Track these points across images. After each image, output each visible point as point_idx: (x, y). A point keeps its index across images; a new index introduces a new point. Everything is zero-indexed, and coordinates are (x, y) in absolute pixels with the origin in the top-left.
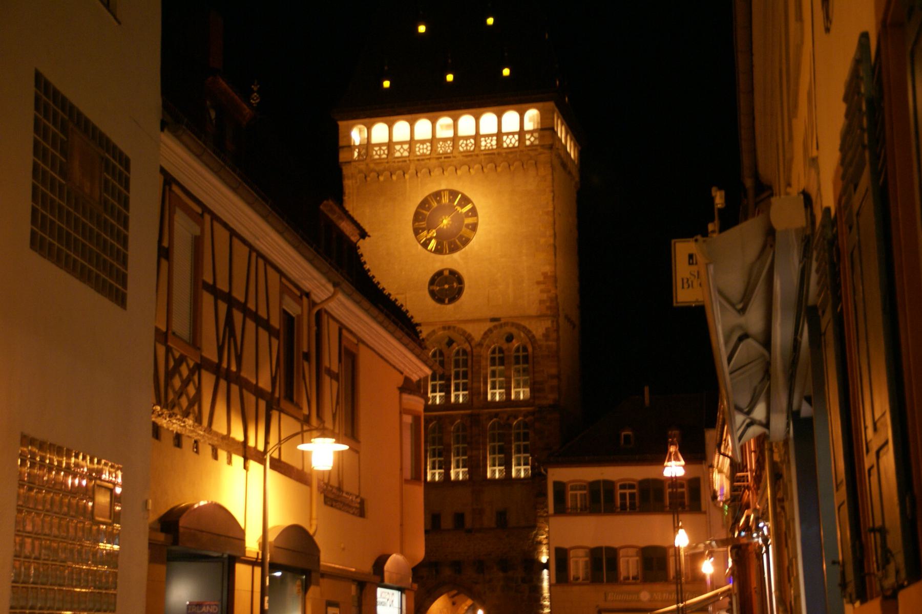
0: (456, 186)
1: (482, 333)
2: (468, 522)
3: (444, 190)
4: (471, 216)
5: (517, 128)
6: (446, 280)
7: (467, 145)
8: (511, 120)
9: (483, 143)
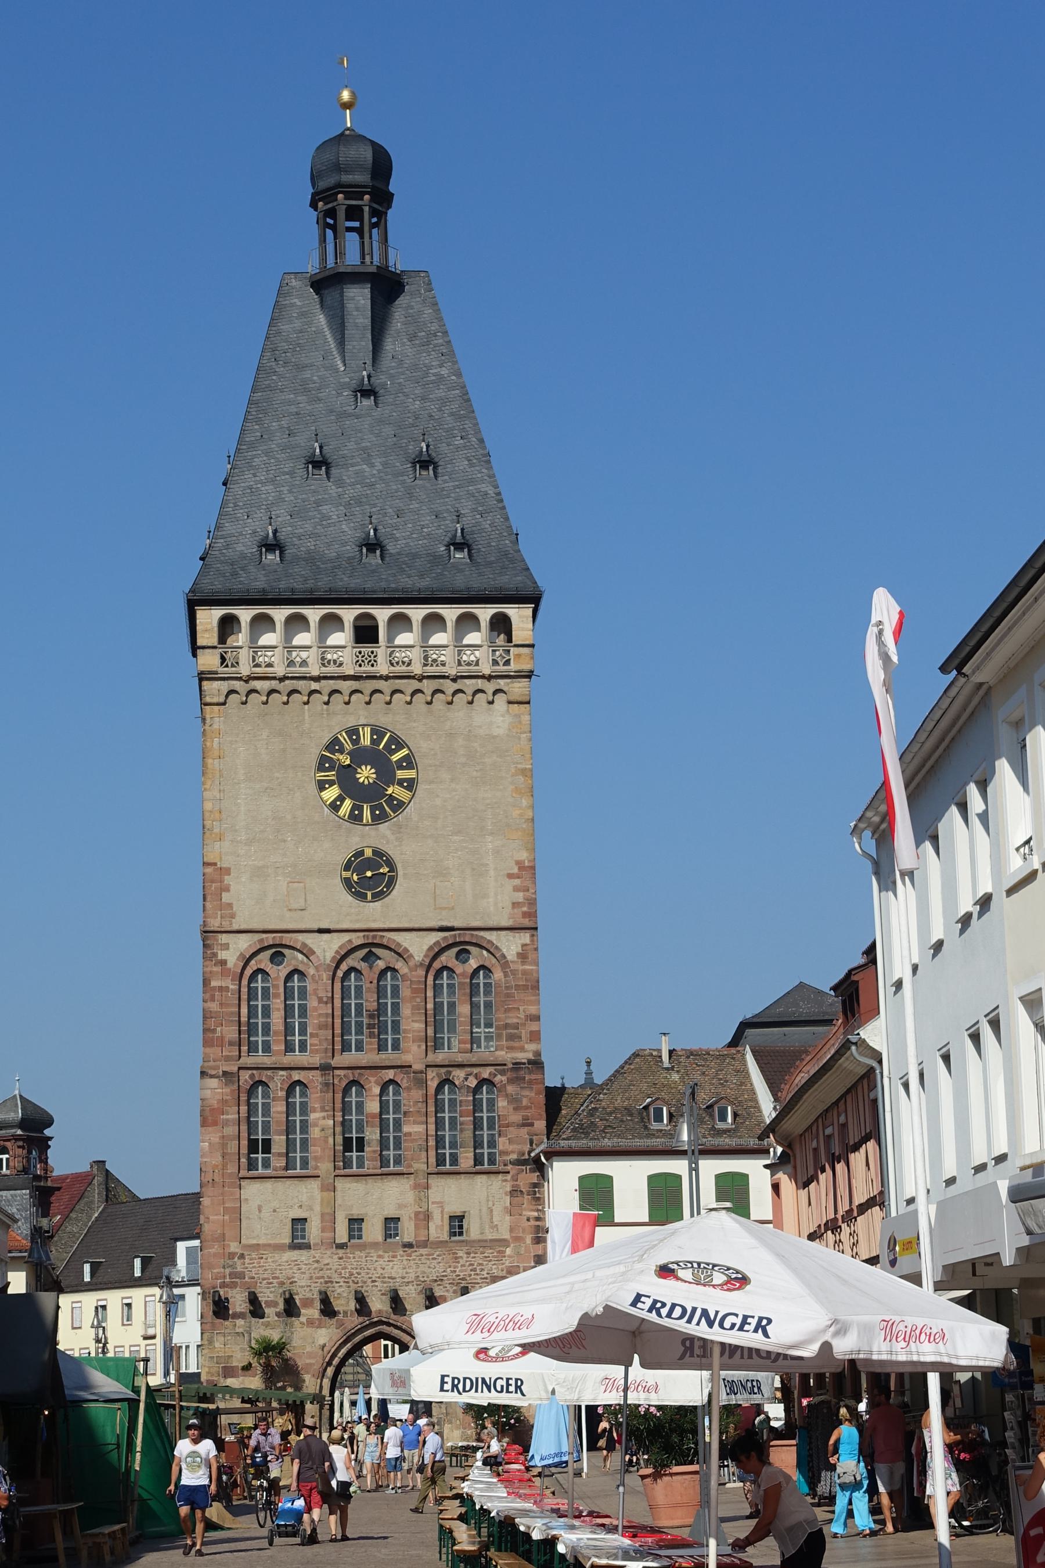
0: (384, 720)
1: (425, 948)
2: (408, 1231)
6: (370, 864)
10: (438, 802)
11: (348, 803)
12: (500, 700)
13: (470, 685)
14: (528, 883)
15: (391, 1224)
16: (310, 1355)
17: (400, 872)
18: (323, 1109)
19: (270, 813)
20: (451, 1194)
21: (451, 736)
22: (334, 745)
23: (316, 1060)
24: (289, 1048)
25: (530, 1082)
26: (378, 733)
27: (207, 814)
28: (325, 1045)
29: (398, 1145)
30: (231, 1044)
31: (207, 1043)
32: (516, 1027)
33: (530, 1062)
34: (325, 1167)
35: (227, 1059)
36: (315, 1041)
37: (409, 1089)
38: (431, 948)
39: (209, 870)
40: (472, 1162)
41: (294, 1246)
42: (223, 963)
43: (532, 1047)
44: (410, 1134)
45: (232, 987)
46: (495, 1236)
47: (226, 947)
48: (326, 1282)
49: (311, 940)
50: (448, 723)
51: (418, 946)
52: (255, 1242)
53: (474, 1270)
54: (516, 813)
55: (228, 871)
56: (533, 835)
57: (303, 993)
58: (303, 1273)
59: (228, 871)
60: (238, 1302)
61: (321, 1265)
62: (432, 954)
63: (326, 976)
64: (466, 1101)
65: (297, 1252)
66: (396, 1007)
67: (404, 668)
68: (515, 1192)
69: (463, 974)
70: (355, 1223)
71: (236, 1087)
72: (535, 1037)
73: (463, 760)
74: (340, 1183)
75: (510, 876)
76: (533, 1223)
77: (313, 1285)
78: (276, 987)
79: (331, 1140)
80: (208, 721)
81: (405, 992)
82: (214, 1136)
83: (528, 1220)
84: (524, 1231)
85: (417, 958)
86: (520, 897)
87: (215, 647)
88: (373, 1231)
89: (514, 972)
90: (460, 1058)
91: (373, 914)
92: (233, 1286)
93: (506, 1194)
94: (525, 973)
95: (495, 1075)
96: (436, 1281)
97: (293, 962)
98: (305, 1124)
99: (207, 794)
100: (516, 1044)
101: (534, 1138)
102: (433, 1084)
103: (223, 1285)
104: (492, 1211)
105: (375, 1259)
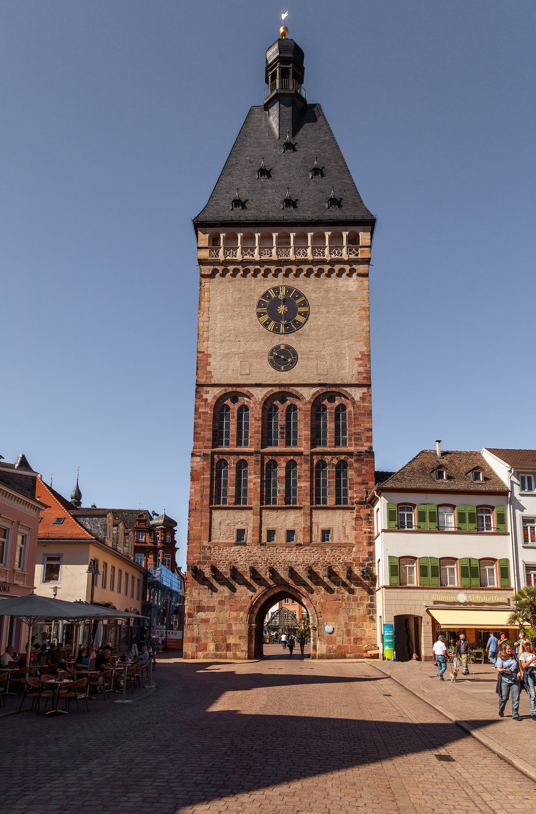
1: (311, 394)
2: (300, 538)
3: (282, 286)
4: (303, 306)
10: (320, 323)
11: (273, 323)
12: (354, 275)
13: (337, 268)
14: (366, 362)
15: (290, 534)
16: (244, 601)
17: (299, 357)
18: (255, 473)
19: (232, 328)
20: (322, 519)
21: (327, 291)
22: (266, 295)
23: (252, 449)
24: (239, 444)
25: (367, 462)
26: (289, 290)
27: (200, 328)
28: (257, 442)
29: (295, 494)
30: (208, 440)
31: (195, 439)
32: (359, 434)
33: (366, 452)
34: (255, 503)
35: (206, 447)
36: (253, 440)
37: (301, 464)
38: (314, 394)
39: (200, 355)
40: (334, 503)
41: (236, 544)
42: (206, 400)
43: (368, 444)
44: (301, 487)
45: (209, 412)
46: (346, 541)
47: (207, 392)
48: (254, 563)
49: (252, 390)
50: (326, 285)
51: (308, 394)
52: (216, 541)
53: (336, 559)
54: (359, 328)
55: (209, 356)
56: (369, 339)
57: (247, 418)
58: (242, 558)
59: (209, 356)
60: (207, 572)
61: (252, 554)
62: (315, 397)
63: (259, 408)
64: (332, 471)
65: (239, 547)
66: (295, 424)
67: (303, 257)
68: (358, 518)
69: (330, 408)
70: (271, 533)
71: (210, 461)
72: (370, 439)
73: (333, 303)
74: (264, 512)
75: (357, 359)
76: (367, 534)
77: (247, 564)
78: (233, 413)
79: (259, 489)
80: (203, 284)
81: (300, 416)
82: (197, 486)
83: (365, 533)
84: (362, 538)
85: (307, 399)
86: (362, 369)
87: (206, 248)
88: (280, 538)
89: (358, 407)
90: (329, 449)
91: (285, 377)
92: (205, 563)
93: (353, 519)
94: (364, 407)
95: (348, 458)
96: (314, 564)
97: (242, 401)
98: (246, 482)
99: (201, 319)
100: (359, 443)
101: (369, 490)
102: (315, 462)
103: (199, 563)
104: (345, 528)
105: (281, 551)
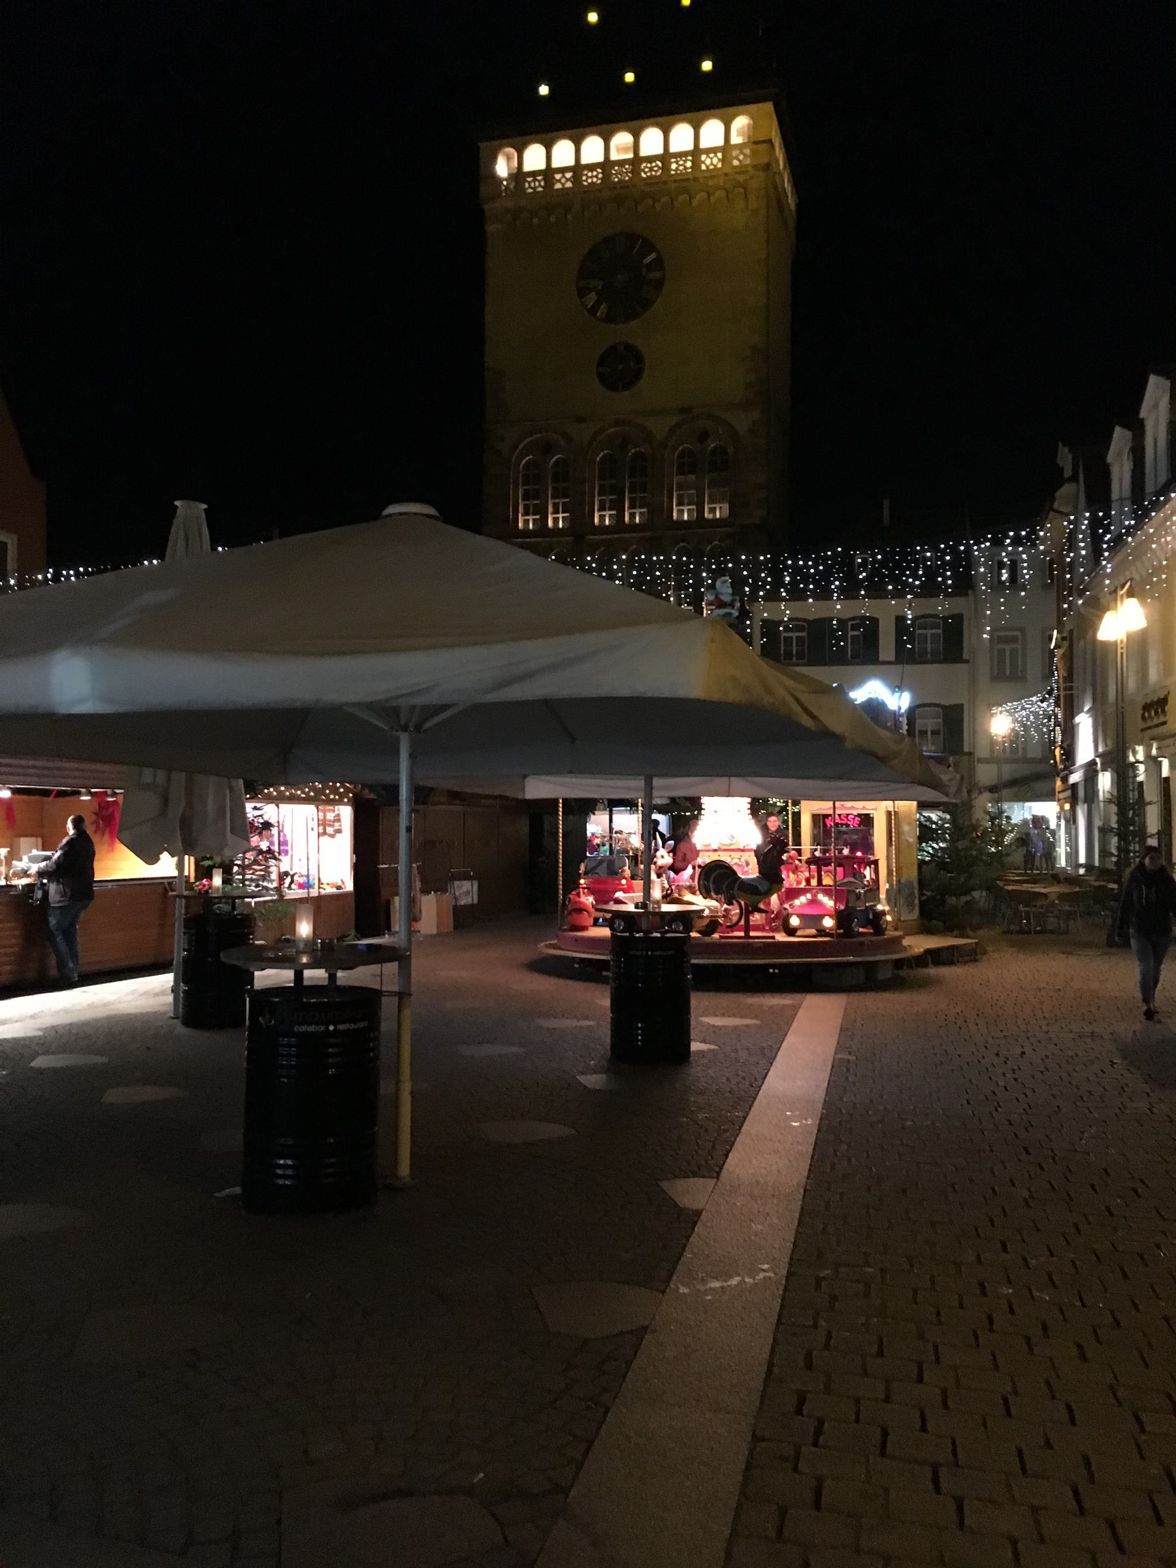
5: (720, 142)
7: (651, 169)
8: (712, 132)
9: (674, 166)
